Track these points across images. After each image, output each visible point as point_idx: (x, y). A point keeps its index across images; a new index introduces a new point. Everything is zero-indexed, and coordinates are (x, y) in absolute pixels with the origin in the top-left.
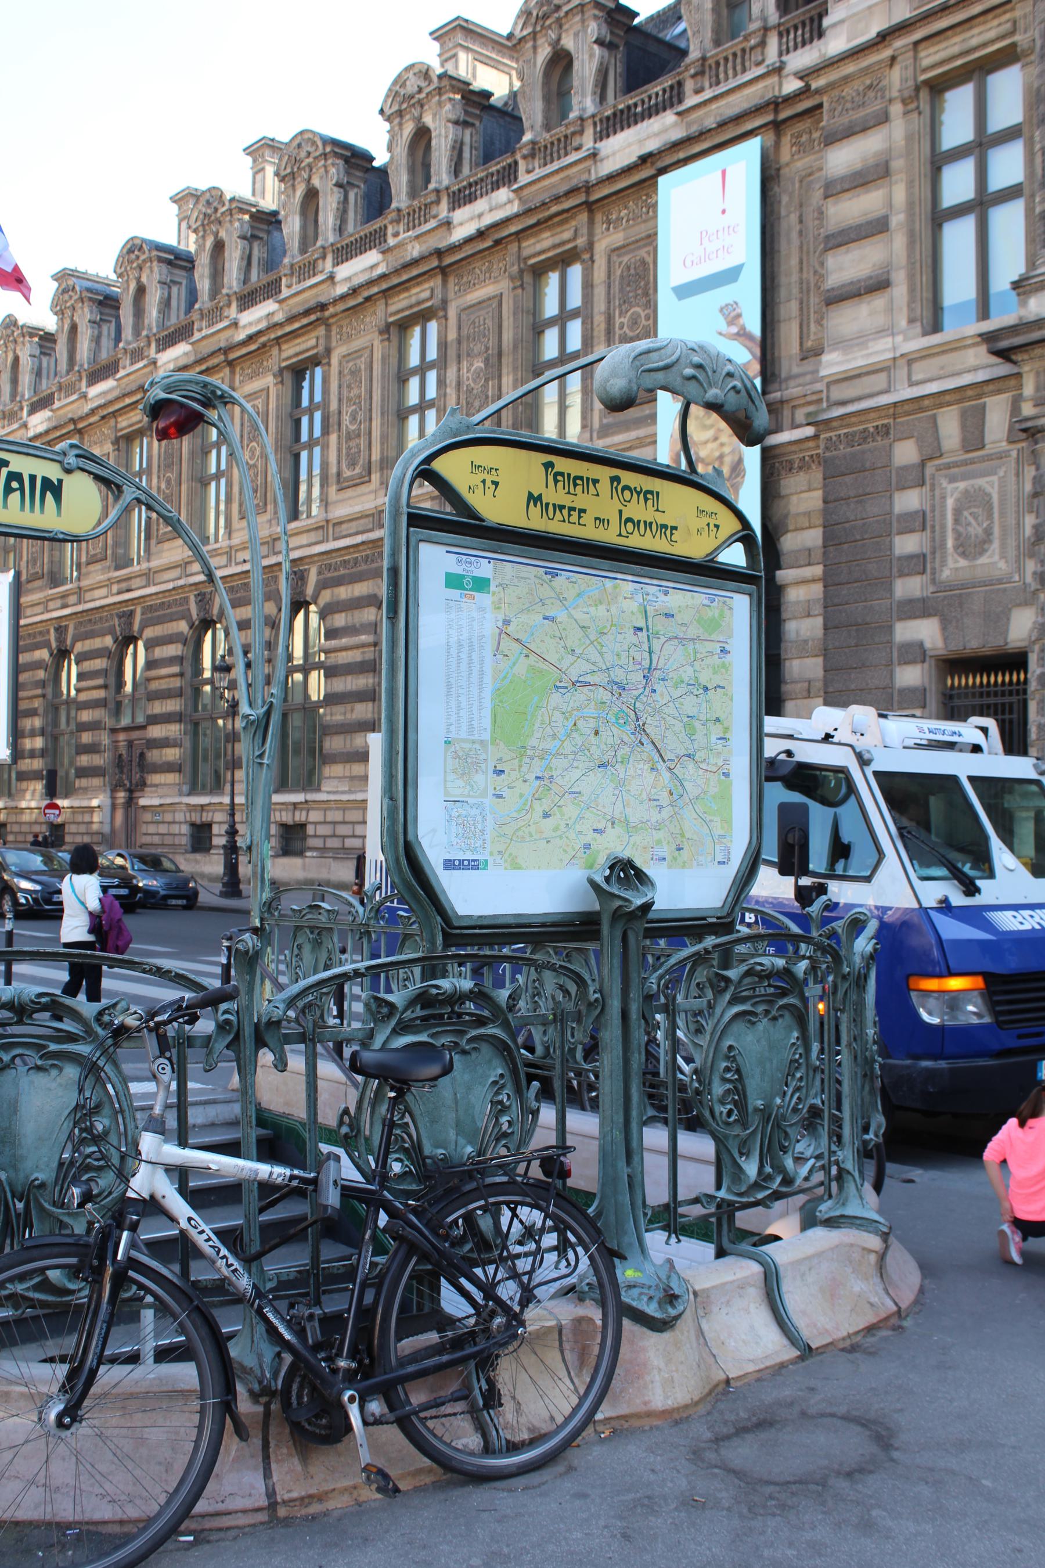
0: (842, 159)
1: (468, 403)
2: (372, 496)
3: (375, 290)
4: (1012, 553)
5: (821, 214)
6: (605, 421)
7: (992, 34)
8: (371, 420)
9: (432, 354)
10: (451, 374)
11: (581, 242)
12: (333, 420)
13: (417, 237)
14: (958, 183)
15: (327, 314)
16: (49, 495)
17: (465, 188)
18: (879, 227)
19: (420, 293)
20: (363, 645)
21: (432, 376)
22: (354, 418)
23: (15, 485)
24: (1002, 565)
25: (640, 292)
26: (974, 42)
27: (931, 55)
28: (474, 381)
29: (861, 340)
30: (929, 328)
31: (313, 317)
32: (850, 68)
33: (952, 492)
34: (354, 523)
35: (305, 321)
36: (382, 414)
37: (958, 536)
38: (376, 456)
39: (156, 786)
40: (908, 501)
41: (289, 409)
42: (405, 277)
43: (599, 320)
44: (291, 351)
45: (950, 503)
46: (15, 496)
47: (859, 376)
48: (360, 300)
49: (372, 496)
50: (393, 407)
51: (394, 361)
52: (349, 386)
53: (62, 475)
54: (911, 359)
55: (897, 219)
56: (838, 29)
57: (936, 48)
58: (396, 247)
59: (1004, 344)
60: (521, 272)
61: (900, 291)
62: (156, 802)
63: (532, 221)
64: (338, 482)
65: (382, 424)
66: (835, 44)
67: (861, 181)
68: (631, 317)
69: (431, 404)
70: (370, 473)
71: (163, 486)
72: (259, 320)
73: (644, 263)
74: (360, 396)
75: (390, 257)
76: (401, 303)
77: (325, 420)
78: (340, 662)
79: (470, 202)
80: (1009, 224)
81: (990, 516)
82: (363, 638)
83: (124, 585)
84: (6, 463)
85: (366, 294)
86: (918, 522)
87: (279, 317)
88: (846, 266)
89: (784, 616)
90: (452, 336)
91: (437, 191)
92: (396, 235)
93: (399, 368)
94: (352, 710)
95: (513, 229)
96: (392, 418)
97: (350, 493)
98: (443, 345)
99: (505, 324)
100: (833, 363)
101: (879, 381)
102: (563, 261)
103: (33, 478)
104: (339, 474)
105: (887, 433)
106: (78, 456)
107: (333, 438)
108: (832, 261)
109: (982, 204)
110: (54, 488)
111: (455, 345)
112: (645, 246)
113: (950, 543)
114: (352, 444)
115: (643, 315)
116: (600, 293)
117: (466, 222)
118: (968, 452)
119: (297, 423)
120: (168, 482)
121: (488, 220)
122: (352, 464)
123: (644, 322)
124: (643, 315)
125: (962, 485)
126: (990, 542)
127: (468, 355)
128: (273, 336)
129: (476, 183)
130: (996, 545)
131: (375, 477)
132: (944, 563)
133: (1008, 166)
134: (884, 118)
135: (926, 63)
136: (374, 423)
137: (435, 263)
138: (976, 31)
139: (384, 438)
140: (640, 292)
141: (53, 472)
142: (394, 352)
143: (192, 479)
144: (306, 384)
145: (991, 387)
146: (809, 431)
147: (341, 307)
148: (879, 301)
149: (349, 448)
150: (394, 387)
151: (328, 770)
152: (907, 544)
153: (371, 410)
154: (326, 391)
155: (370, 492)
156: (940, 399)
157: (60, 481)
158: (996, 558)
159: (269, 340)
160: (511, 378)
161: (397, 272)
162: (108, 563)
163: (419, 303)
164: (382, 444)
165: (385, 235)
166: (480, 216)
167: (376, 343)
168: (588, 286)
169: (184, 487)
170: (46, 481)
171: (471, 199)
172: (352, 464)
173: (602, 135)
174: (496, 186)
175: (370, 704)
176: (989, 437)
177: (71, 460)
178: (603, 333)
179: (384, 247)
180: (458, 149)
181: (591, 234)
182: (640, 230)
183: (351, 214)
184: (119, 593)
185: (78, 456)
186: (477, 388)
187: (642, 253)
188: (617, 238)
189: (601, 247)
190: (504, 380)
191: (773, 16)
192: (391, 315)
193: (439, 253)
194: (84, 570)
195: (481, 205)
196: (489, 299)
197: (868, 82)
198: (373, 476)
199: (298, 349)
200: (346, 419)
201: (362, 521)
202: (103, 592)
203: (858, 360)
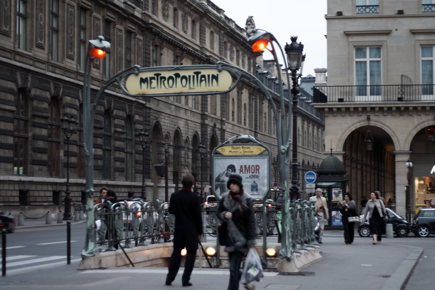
16: (214, 80)
46: (203, 82)
84: (200, 73)
103: (209, 76)
106: (222, 66)
141: (215, 72)
157: (218, 75)
177: (220, 68)
185: (222, 66)
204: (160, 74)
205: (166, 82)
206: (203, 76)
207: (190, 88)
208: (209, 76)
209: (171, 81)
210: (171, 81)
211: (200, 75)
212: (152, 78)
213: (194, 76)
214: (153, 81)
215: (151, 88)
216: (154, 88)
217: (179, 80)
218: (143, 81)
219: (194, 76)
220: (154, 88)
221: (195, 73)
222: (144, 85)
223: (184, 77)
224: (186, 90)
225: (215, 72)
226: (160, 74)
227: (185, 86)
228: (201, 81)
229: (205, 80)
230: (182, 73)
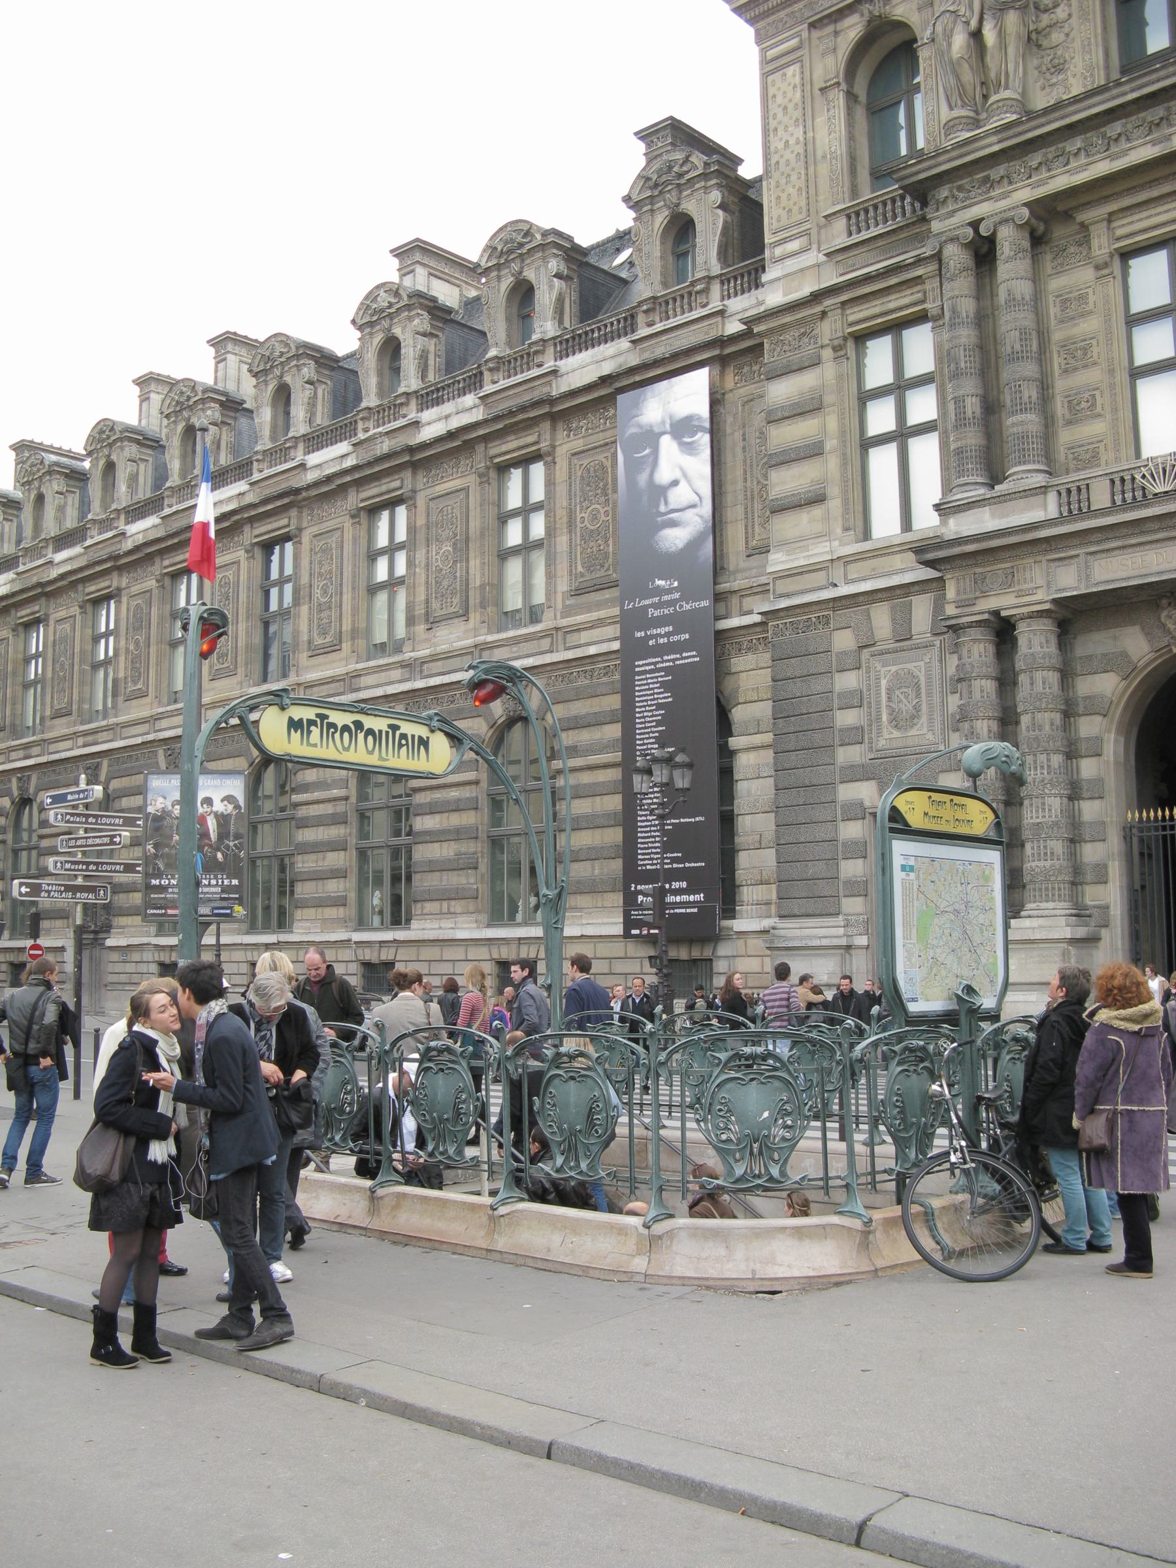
0: (781, 391)
1: (437, 582)
2: (344, 662)
3: (348, 478)
4: (937, 725)
5: (763, 436)
6: (568, 603)
7: (906, 301)
8: (341, 594)
9: (401, 535)
10: (420, 556)
11: (544, 445)
12: (304, 592)
13: (387, 433)
14: (881, 417)
15: (300, 497)
17: (432, 392)
18: (814, 451)
19: (391, 484)
20: (335, 799)
21: (401, 559)
22: (325, 592)
23: (404, 742)
24: (930, 736)
25: (599, 491)
26: (892, 306)
27: (856, 313)
28: (443, 562)
29: (801, 541)
30: (861, 536)
31: (286, 500)
32: (787, 319)
33: (885, 673)
34: (325, 687)
35: (279, 503)
36: (354, 588)
37: (891, 711)
38: (347, 626)
39: (123, 927)
40: (847, 681)
41: (259, 582)
42: (377, 469)
43: (561, 514)
44: (264, 529)
45: (884, 682)
47: (801, 573)
48: (333, 486)
49: (344, 662)
50: (363, 584)
51: (364, 542)
52: (320, 562)
53: (429, 734)
55: (830, 444)
56: (776, 284)
57: (860, 308)
58: (365, 440)
59: (930, 556)
60: (488, 468)
61: (835, 504)
62: (123, 942)
63: (500, 426)
64: (309, 649)
65: (353, 598)
66: (774, 297)
67: (799, 411)
68: (591, 513)
69: (401, 581)
70: (341, 642)
71: (131, 647)
72: (230, 499)
73: (603, 467)
74: (330, 572)
75: (360, 450)
76: (372, 492)
77: (296, 591)
78: (312, 814)
79: (438, 405)
80: (926, 454)
81: (918, 695)
82: (335, 793)
83: (90, 739)
84: (398, 728)
85: (339, 482)
86: (855, 700)
87: (250, 499)
88: (788, 481)
89: (736, 777)
90: (421, 521)
91: (407, 394)
92: (366, 430)
93: (369, 548)
94: (324, 858)
95: (481, 432)
96: (363, 592)
97: (321, 659)
98: (412, 529)
99: (472, 514)
100: (778, 561)
101: (820, 578)
102: (525, 462)
103: (413, 736)
104: (309, 642)
105: (828, 623)
107: (304, 609)
108: (775, 475)
109: (902, 435)
110: (424, 743)
111: (424, 530)
112: (603, 452)
113: (885, 718)
114: (324, 614)
115: (602, 511)
116: (561, 490)
117: (434, 423)
118: (898, 641)
119: (267, 594)
120: (137, 643)
121: (455, 423)
122: (324, 633)
123: (603, 518)
124: (602, 511)
125: (894, 669)
126: (919, 717)
127: (437, 540)
128: (246, 515)
129: (443, 388)
130: (924, 719)
131: (346, 646)
132: (879, 733)
133: (923, 406)
134: (816, 363)
135: (851, 318)
136: (345, 597)
137: (407, 458)
138: (892, 297)
139: (355, 611)
140: (599, 491)
141: (423, 731)
142: (363, 534)
143: (160, 642)
144: (275, 558)
145: (916, 588)
146: (757, 618)
147: (314, 492)
148: (817, 511)
149: (320, 619)
150: (363, 564)
151: (299, 914)
152: (847, 718)
153: (341, 585)
154: (296, 566)
155: (341, 660)
156: (873, 596)
158: (925, 731)
159: (242, 519)
160: (478, 561)
161: (370, 464)
162: (72, 718)
163: (389, 492)
164: (353, 615)
165: (355, 429)
166: (447, 417)
167: (346, 525)
168: (550, 483)
169: (153, 649)
170: (420, 737)
171: (438, 402)
172: (324, 633)
173: (562, 355)
174: (463, 392)
175: (342, 853)
176: (915, 630)
178: (565, 526)
179: (354, 440)
180: (423, 357)
181: (553, 439)
182: (599, 438)
183: (319, 408)
184: (85, 746)
186: (446, 569)
187: (601, 457)
188: (578, 444)
189: (562, 452)
190: (472, 563)
191: (716, 269)
192: (362, 501)
193: (411, 450)
194: (48, 723)
195: (447, 408)
196: (457, 491)
197: (802, 330)
198: (344, 645)
199: (269, 527)
200: (317, 592)
201: (333, 685)
202: (68, 744)
203: (801, 560)
204: (327, 717)
205: (337, 735)
206: (404, 736)
207: (381, 758)
208: (413, 736)
209: (346, 735)
210: (346, 735)
211: (398, 733)
212: (311, 723)
213: (387, 733)
214: (313, 728)
215: (309, 744)
216: (315, 745)
217: (361, 736)
218: (294, 725)
219: (387, 733)
220: (315, 745)
221: (390, 726)
222: (296, 736)
223: (370, 732)
224: (373, 760)
225: (423, 731)
226: (327, 717)
227: (371, 753)
228: (401, 746)
229: (407, 744)
230: (369, 722)
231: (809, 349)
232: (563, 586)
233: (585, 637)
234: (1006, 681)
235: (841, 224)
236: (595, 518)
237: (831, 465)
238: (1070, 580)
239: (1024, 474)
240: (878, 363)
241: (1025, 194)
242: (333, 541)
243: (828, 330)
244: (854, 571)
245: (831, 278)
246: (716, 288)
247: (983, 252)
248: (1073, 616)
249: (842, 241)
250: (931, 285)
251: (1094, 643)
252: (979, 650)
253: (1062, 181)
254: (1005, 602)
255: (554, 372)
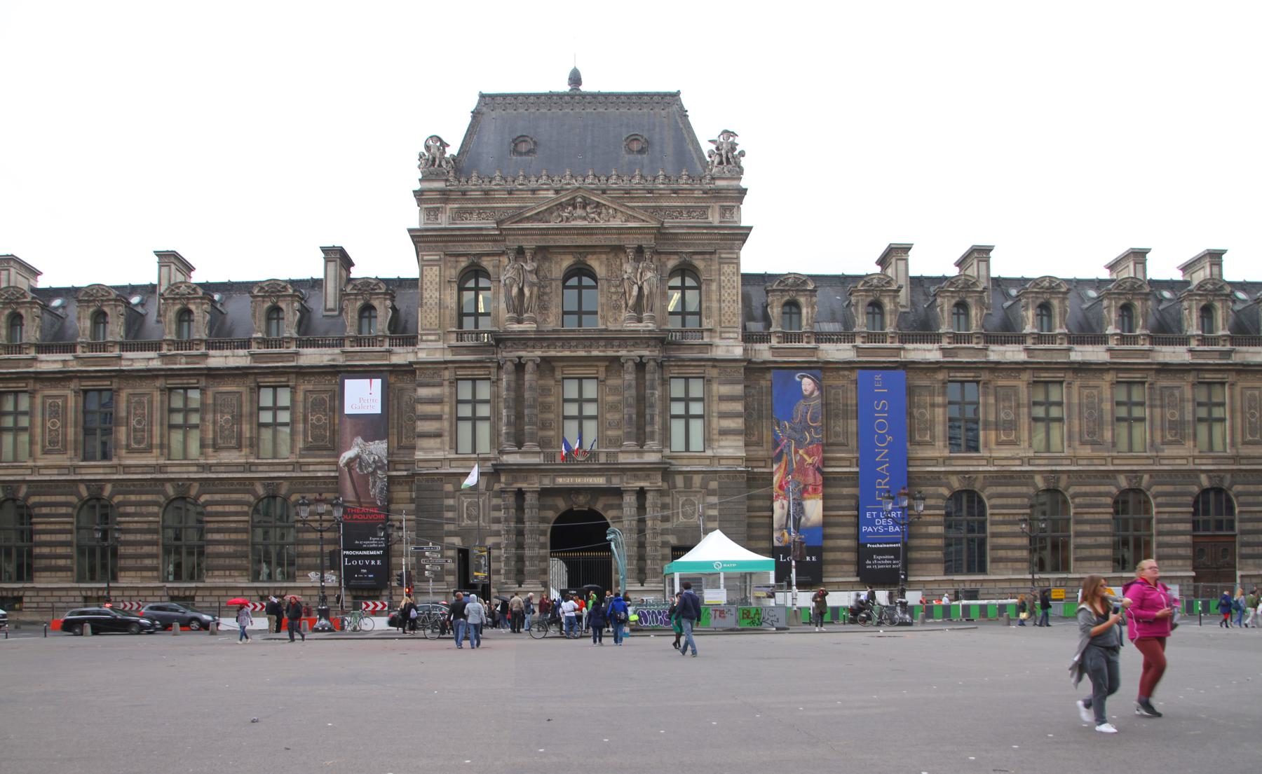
0: (423, 392)
18: (438, 418)
29: (431, 450)
40: (451, 502)
54: (451, 460)
55: (445, 416)
66: (423, 356)
80: (484, 429)
86: (450, 508)
88: (423, 426)
100: (419, 455)
101: (438, 464)
108: (419, 423)
134: (441, 385)
148: (438, 440)
152: (450, 515)
172: (139, 443)
188: (310, 387)
231: (437, 380)
232: (300, 444)
233: (312, 468)
234: (520, 508)
235: (454, 336)
236: (319, 420)
237: (446, 424)
238: (547, 483)
239: (528, 445)
240: (465, 391)
241: (538, 353)
242: (145, 400)
243: (447, 374)
244: (453, 464)
245: (449, 357)
246: (387, 342)
247: (520, 367)
248: (544, 493)
249: (454, 343)
250: (494, 370)
251: (549, 501)
252: (511, 500)
253: (552, 353)
254: (524, 486)
255: (297, 354)
